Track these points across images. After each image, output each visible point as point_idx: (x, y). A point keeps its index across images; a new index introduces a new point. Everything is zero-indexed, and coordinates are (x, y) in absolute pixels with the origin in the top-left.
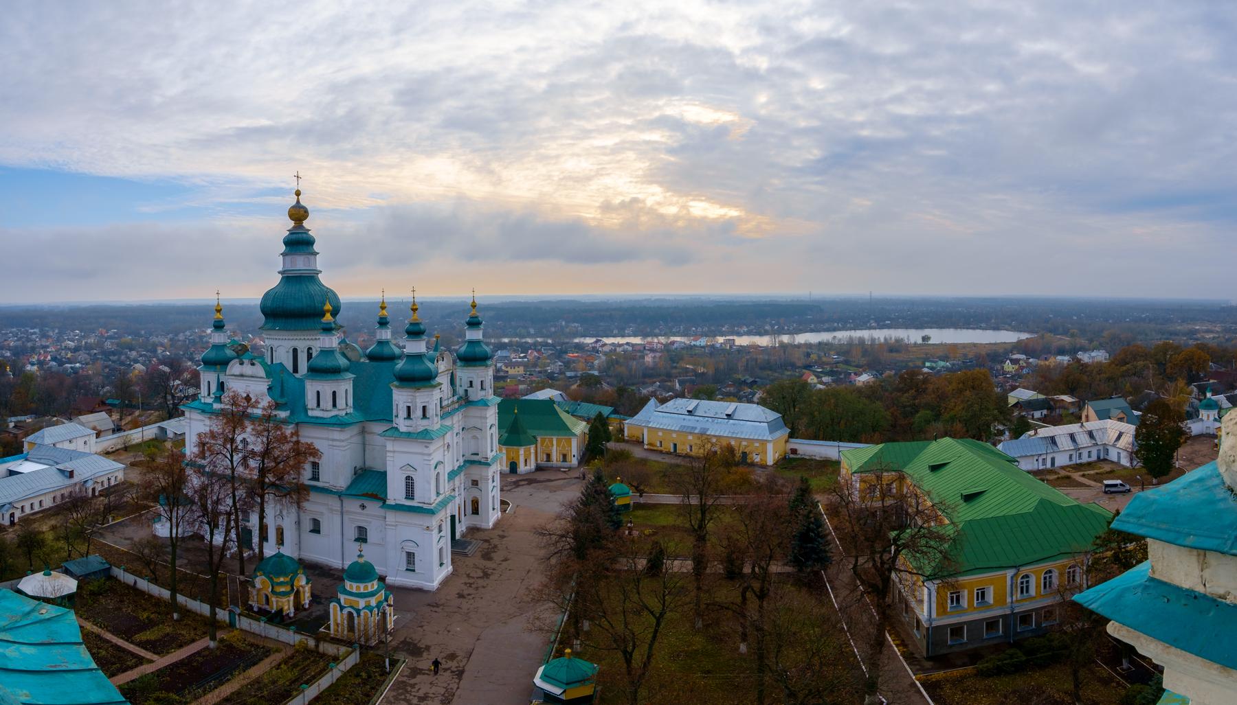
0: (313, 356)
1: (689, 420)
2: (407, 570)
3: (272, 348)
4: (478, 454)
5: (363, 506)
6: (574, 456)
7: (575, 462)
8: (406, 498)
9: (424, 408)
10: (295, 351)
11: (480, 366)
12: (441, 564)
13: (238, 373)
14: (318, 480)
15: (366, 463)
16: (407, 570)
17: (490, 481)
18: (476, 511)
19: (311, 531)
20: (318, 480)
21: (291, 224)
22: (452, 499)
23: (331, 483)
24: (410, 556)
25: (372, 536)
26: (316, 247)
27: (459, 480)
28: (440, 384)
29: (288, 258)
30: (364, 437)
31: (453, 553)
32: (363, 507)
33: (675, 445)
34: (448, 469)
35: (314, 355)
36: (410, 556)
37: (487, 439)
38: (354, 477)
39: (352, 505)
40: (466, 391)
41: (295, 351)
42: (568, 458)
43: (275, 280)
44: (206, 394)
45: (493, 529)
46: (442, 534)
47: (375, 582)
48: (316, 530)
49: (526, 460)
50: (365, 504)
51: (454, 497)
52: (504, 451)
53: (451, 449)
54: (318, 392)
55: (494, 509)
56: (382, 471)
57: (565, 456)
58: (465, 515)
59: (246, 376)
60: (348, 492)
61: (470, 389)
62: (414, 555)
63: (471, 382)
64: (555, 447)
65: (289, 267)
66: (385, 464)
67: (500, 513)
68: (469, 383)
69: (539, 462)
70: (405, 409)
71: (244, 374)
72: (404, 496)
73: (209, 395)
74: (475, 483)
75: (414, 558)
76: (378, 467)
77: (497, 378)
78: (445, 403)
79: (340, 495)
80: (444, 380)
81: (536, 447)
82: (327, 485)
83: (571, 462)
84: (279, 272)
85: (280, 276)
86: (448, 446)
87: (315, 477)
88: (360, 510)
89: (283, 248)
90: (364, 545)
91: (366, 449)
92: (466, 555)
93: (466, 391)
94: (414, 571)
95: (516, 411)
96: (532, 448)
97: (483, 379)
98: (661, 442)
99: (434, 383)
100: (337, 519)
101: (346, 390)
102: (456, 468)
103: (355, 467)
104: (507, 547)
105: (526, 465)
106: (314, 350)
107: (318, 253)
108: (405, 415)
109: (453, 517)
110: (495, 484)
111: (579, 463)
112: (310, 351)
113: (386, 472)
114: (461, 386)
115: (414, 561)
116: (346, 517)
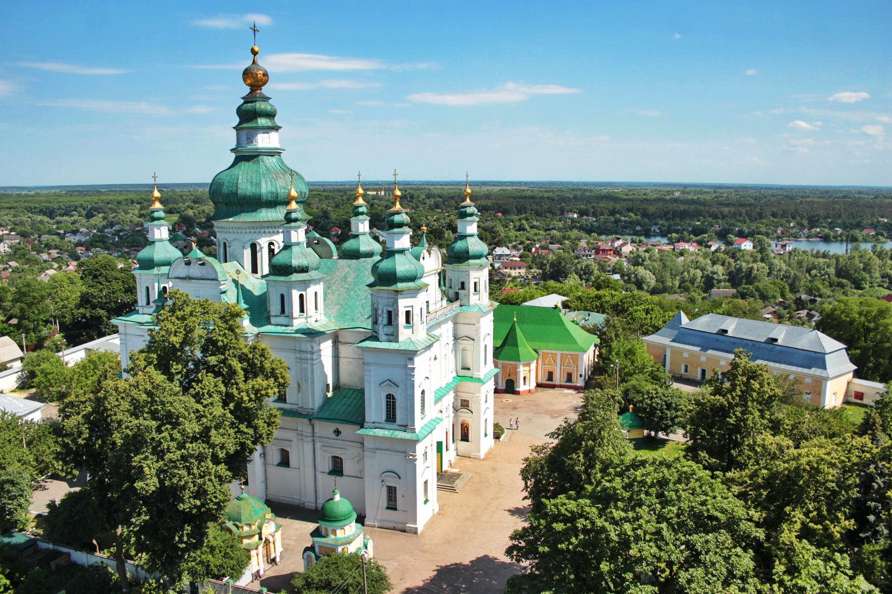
0: (276, 253)
1: (724, 342)
2: (388, 508)
3: (225, 244)
4: (469, 369)
5: (338, 432)
6: (581, 376)
7: (580, 383)
8: (386, 421)
9: (408, 313)
12: (426, 501)
13: (183, 275)
16: (388, 508)
17: (483, 400)
18: (465, 438)
19: (279, 465)
22: (438, 421)
23: (300, 405)
24: (392, 492)
25: (348, 467)
26: (278, 121)
27: (449, 399)
28: (427, 285)
29: (244, 134)
31: (439, 487)
32: (337, 432)
33: (704, 372)
35: (276, 251)
36: (392, 492)
39: (325, 429)
40: (457, 294)
41: (254, 247)
42: (574, 378)
44: (145, 303)
45: (484, 460)
46: (428, 463)
47: (354, 524)
48: (285, 462)
49: (525, 378)
50: (340, 429)
51: (441, 420)
52: (500, 366)
54: (282, 296)
55: (486, 435)
57: (569, 377)
58: (454, 441)
59: (194, 279)
60: (320, 415)
61: (461, 292)
62: (395, 490)
63: (463, 284)
64: (559, 365)
67: (493, 440)
68: (460, 284)
69: (540, 381)
70: (385, 315)
71: (191, 275)
72: (384, 417)
73: (148, 303)
74: (465, 404)
75: (395, 494)
77: (491, 280)
78: (431, 309)
79: (311, 417)
80: (432, 281)
81: (537, 363)
82: (295, 407)
83: (577, 382)
84: (232, 150)
86: (435, 359)
88: (334, 436)
90: (338, 478)
91: (341, 364)
92: (453, 490)
94: (395, 509)
95: (515, 319)
96: (533, 365)
97: (477, 280)
98: (686, 366)
99: (418, 283)
100: (308, 447)
101: (316, 293)
104: (499, 482)
105: (525, 384)
106: (276, 245)
107: (280, 127)
108: (385, 321)
109: (439, 444)
110: (488, 405)
111: (586, 383)
112: (272, 247)
113: (363, 389)
114: (451, 288)
115: (395, 497)
116: (318, 445)
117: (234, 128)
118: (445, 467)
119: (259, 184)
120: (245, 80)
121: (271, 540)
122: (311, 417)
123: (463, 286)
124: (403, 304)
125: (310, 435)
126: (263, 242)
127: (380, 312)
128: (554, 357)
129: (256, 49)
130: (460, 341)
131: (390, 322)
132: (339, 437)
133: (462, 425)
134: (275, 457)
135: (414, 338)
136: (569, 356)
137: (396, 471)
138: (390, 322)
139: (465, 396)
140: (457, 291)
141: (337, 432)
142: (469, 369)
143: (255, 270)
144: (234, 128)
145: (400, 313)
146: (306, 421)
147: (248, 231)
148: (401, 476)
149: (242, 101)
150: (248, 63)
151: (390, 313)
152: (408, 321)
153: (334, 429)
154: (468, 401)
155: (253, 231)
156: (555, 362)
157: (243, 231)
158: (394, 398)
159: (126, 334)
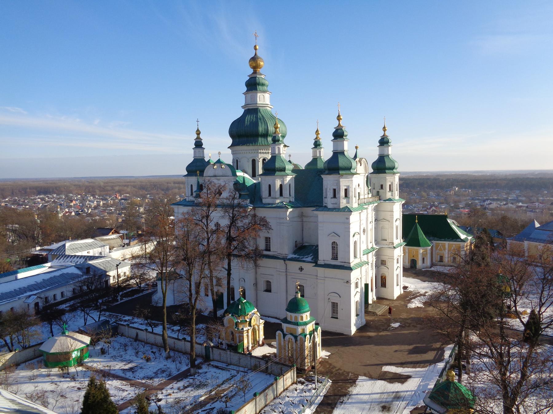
2: (332, 317)
3: (237, 161)
5: (301, 269)
11: (388, 173)
13: (212, 175)
14: (270, 250)
15: (305, 240)
20: (270, 250)
26: (269, 89)
30: (302, 220)
32: (301, 269)
34: (364, 247)
37: (393, 228)
38: (295, 248)
40: (378, 192)
41: (254, 162)
43: (240, 113)
50: (303, 267)
53: (366, 233)
56: (316, 245)
61: (381, 191)
62: (337, 306)
66: (317, 240)
71: (217, 175)
75: (337, 308)
76: (313, 242)
87: (268, 249)
88: (299, 271)
89: (245, 89)
91: (304, 230)
93: (378, 192)
94: (337, 318)
102: (369, 248)
103: (296, 242)
113: (317, 246)
114: (374, 189)
115: (337, 310)
116: (289, 277)
118: (370, 302)
121: (256, 327)
122: (285, 259)
123: (382, 187)
124: (344, 183)
125: (284, 271)
127: (328, 190)
128: (444, 246)
129: (257, 47)
130: (380, 222)
131: (335, 196)
132: (302, 272)
133: (382, 277)
134: (262, 286)
135: (349, 206)
136: (454, 246)
137: (338, 293)
138: (335, 196)
139: (384, 258)
140: (378, 190)
141: (301, 269)
142: (386, 240)
145: (341, 189)
146: (283, 261)
147: (251, 152)
148: (341, 296)
149: (249, 78)
150: (253, 55)
151: (335, 190)
152: (346, 196)
153: (299, 267)
154: (385, 261)
155: (253, 152)
156: (445, 249)
157: (248, 152)
158: (337, 245)
159: (178, 213)
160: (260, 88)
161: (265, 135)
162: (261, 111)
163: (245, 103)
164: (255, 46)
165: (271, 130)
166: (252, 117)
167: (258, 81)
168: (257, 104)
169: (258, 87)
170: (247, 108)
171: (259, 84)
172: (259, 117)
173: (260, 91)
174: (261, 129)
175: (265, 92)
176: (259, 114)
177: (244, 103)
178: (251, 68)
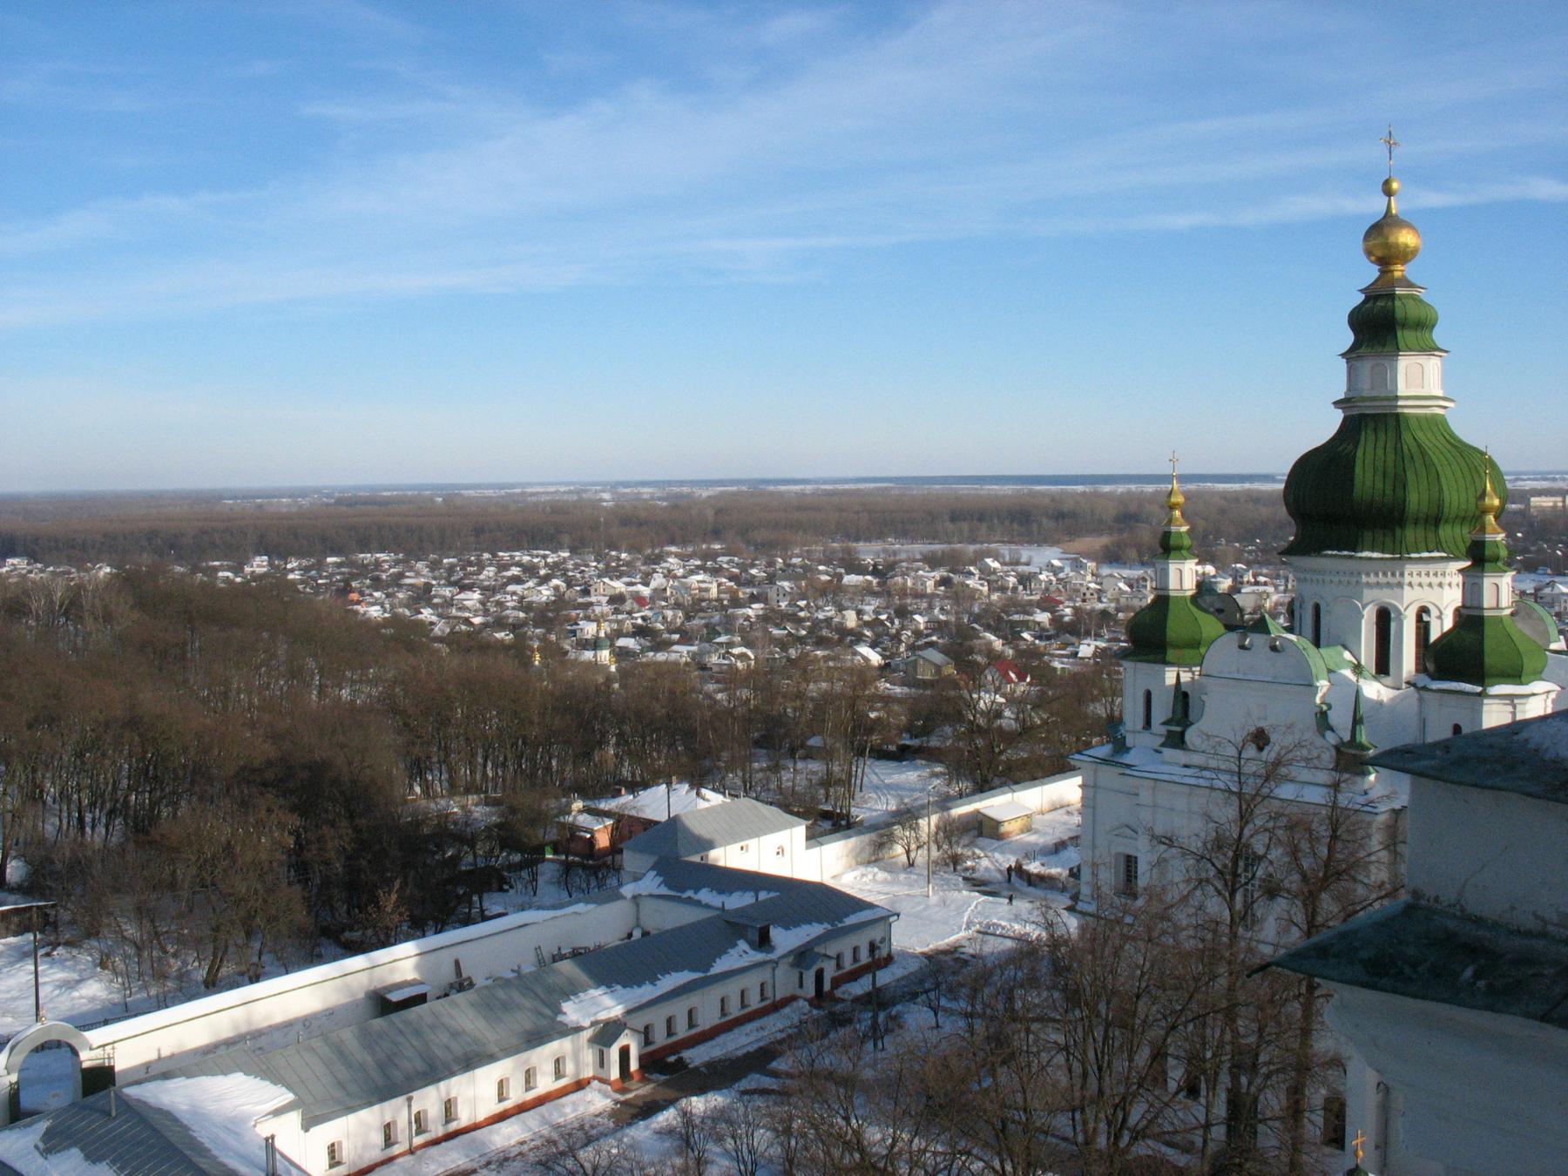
3: (1317, 608)
10: (1384, 618)
21: (1371, 273)
26: (1439, 335)
29: (1366, 367)
41: (1384, 618)
43: (1324, 426)
65: (1366, 388)
84: (1337, 404)
85: (1338, 417)
89: (1348, 338)
106: (1434, 612)
112: (1425, 618)
117: (1343, 355)
119: (1400, 483)
120: (1369, 253)
126: (1408, 602)
129: (1395, 185)
143: (1383, 666)
144: (1343, 355)
149: (1363, 297)
160: (1404, 336)
161: (1435, 519)
162: (1413, 424)
163: (1349, 389)
164: (1387, 183)
165: (1455, 498)
166: (1380, 452)
167: (1399, 314)
168: (1397, 398)
169: (1399, 334)
170: (1355, 412)
171: (1405, 325)
172: (1405, 447)
173: (1411, 350)
174: (1416, 499)
175: (1430, 349)
176: (1406, 437)
177: (1344, 388)
178: (1372, 262)
